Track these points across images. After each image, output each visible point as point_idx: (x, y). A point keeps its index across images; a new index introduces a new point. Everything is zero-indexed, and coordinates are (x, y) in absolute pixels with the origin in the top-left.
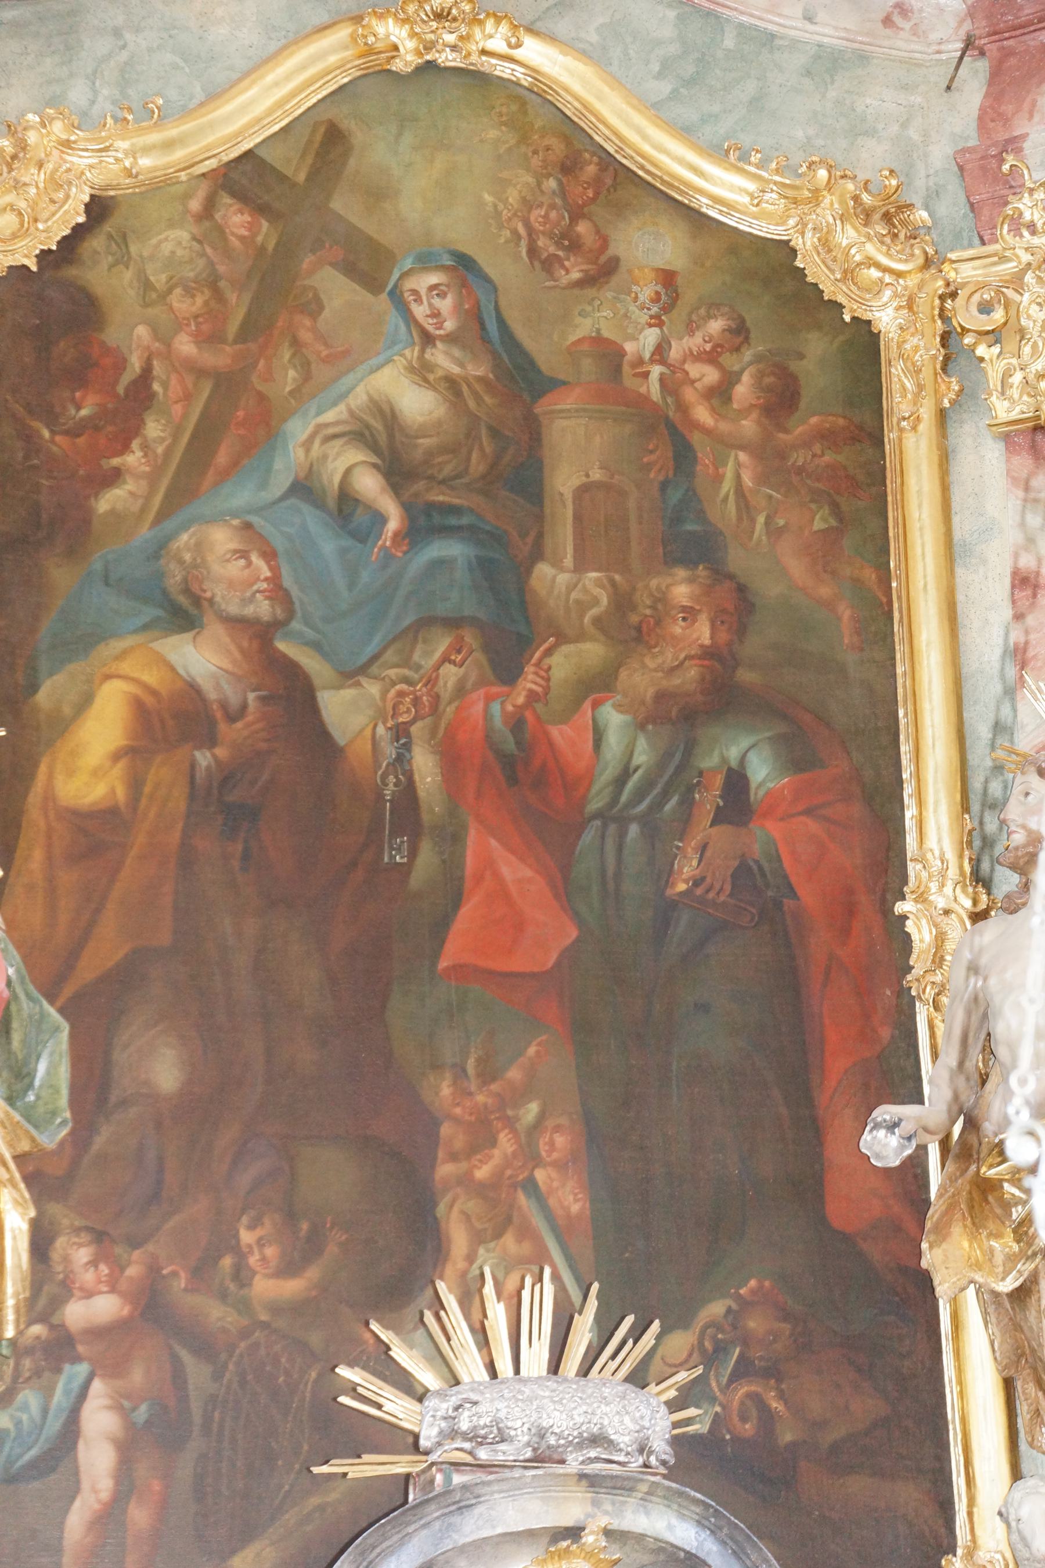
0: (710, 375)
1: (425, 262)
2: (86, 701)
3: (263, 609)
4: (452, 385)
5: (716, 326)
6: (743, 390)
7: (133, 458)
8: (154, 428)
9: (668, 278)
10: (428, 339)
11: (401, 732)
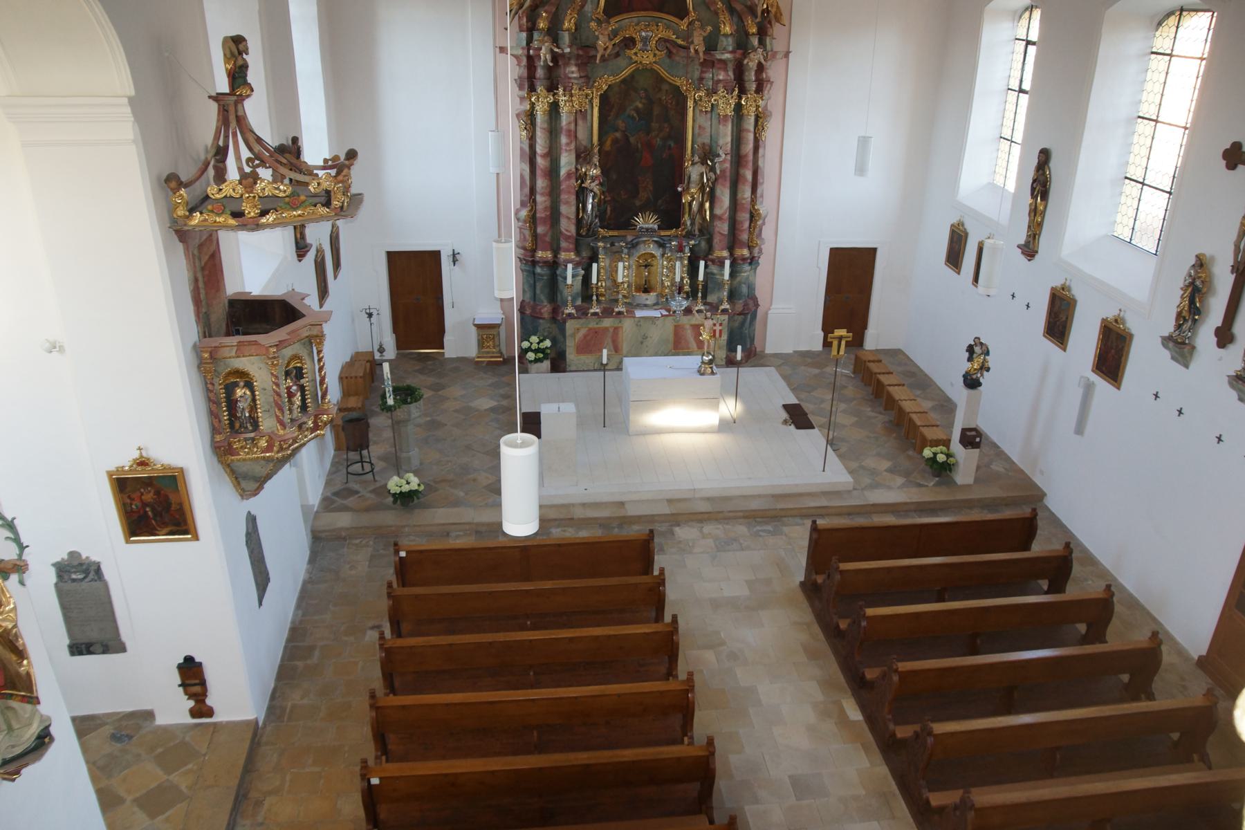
0: (670, 101)
1: (642, 90)
2: (607, 140)
3: (624, 129)
4: (644, 104)
5: (671, 96)
6: (674, 103)
7: (612, 114)
8: (614, 110)
9: (667, 91)
10: (641, 98)
11: (637, 142)
